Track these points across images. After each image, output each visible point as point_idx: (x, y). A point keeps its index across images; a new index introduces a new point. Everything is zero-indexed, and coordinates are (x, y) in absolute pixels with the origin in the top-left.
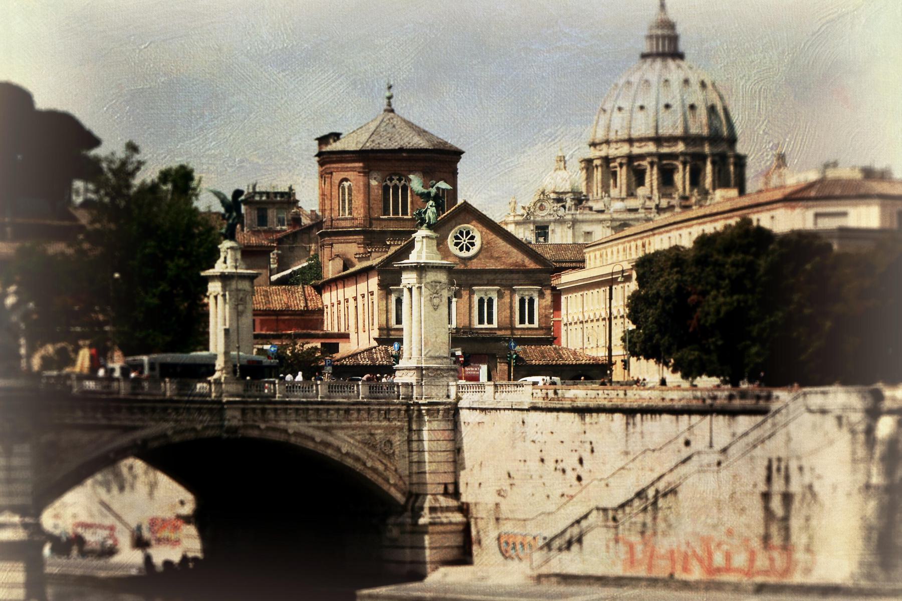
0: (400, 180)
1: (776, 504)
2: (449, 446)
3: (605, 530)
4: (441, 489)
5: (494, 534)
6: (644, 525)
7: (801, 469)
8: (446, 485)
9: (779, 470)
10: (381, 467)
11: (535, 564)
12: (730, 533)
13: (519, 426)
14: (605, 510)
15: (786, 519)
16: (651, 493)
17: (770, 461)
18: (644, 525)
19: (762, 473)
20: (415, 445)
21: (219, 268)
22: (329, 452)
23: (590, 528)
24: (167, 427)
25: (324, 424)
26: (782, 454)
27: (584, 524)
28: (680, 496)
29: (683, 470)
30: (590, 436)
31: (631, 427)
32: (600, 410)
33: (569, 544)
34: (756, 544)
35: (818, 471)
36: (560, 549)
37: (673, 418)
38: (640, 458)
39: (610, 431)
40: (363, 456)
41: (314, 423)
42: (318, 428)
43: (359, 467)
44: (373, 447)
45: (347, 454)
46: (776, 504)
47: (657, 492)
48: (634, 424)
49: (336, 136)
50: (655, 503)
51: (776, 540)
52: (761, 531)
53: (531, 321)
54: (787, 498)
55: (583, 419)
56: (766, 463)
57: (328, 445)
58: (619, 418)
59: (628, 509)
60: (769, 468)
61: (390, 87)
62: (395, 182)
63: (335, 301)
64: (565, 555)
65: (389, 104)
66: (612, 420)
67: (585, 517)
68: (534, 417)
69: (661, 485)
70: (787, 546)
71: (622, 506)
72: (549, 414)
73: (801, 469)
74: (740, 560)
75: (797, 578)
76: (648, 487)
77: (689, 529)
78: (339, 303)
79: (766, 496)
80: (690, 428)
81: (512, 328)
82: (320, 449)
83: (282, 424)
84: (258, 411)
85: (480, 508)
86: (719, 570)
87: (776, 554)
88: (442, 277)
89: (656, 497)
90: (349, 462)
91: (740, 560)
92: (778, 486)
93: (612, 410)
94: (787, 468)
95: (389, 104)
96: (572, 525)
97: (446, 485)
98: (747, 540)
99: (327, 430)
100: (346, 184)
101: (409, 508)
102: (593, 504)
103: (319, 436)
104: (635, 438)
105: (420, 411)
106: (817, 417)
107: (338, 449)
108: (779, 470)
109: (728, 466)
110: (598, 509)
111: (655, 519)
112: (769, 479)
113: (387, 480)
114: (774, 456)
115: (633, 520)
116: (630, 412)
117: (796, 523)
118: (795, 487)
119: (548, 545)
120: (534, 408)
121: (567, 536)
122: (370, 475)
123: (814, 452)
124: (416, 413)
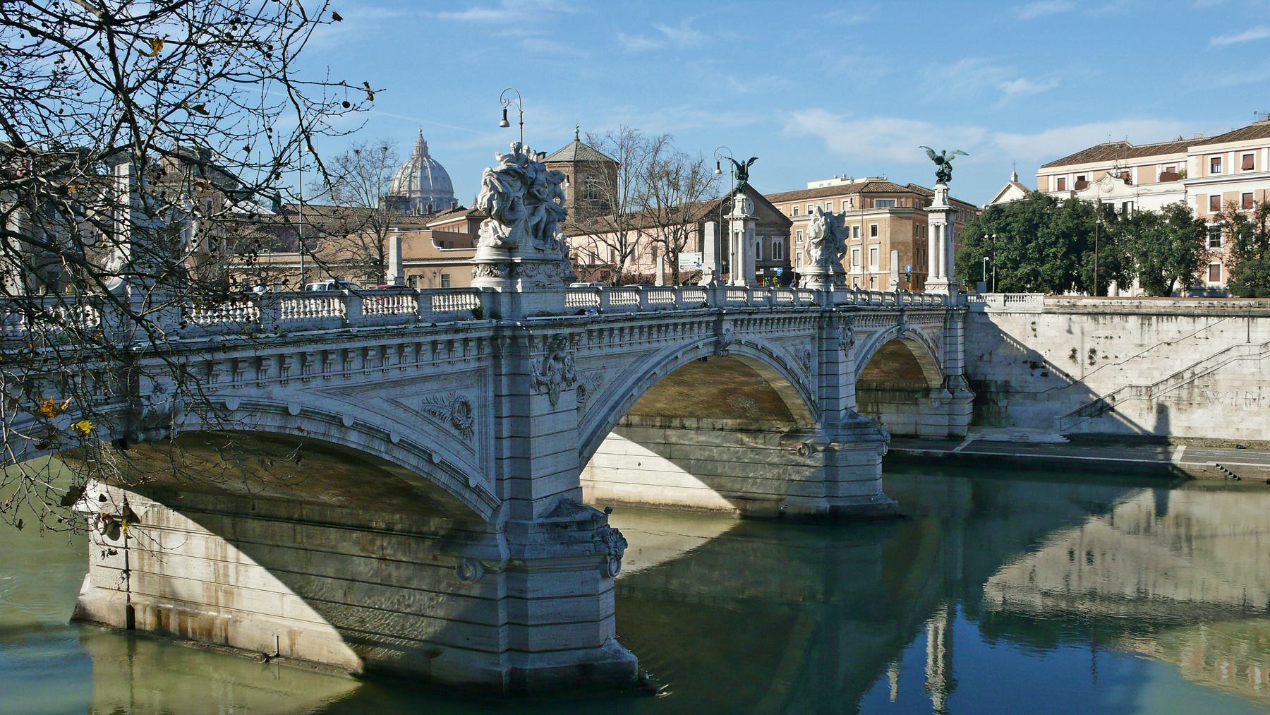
16: (1187, 375)
28: (1217, 377)
29: (1223, 358)
31: (1146, 327)
36: (1091, 416)
47: (1193, 374)
49: (544, 154)
55: (1096, 320)
58: (1132, 319)
59: (1162, 387)
64: (1094, 420)
69: (1198, 370)
72: (1061, 317)
80: (1208, 328)
102: (1126, 382)
110: (1131, 387)
111: (1191, 394)
119: (1079, 413)
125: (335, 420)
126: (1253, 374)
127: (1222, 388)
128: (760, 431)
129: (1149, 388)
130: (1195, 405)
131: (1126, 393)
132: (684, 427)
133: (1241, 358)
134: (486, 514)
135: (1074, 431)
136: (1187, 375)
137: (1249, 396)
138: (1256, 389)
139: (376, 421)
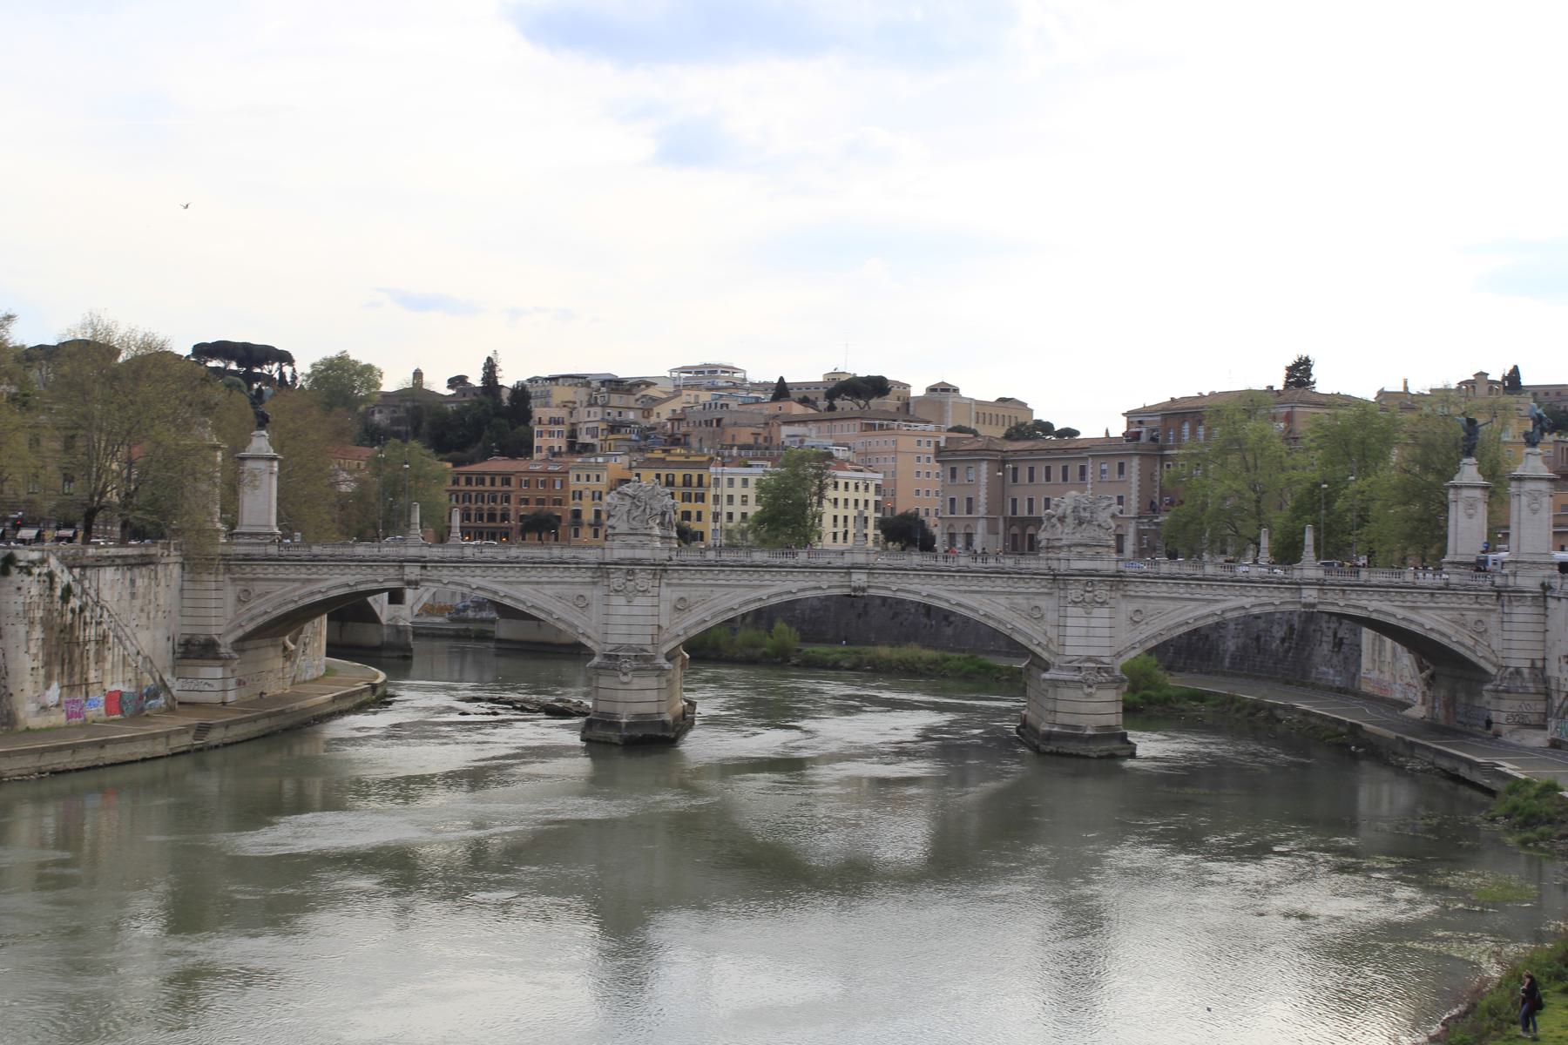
2: (1540, 628)
4: (1528, 663)
8: (1533, 661)
10: (1470, 643)
21: (1457, 481)
22: (1413, 628)
24: (1246, 601)
43: (1445, 641)
44: (1464, 625)
57: (1412, 621)
82: (1404, 625)
83: (1363, 603)
88: (1544, 486)
97: (1533, 661)
99: (1412, 608)
103: (1401, 613)
107: (1422, 625)
113: (1474, 652)
122: (1456, 648)
125: (496, 593)
134: (596, 648)
139: (523, 597)
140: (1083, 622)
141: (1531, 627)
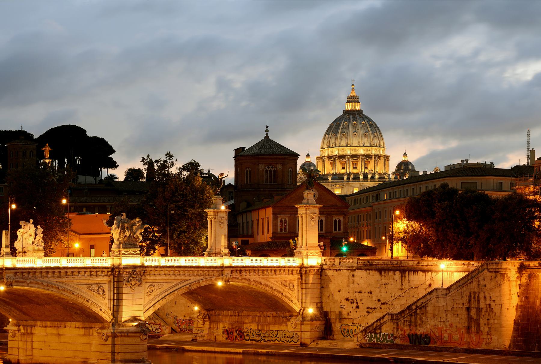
0: (272, 168)
1: (473, 313)
3: (392, 324)
5: (339, 325)
6: (410, 321)
7: (485, 297)
9: (474, 298)
10: (289, 296)
11: (359, 340)
12: (451, 325)
13: (351, 278)
14: (392, 315)
15: (478, 320)
16: (414, 307)
17: (470, 293)
18: (410, 321)
19: (466, 298)
20: (304, 286)
23: (385, 323)
25: (265, 276)
26: (476, 290)
27: (382, 321)
28: (428, 308)
29: (429, 297)
30: (384, 281)
32: (389, 270)
33: (375, 329)
34: (463, 331)
35: (493, 299)
37: (424, 274)
38: (408, 291)
39: (394, 279)
40: (282, 291)
41: (261, 276)
42: (263, 278)
45: (275, 290)
46: (473, 313)
47: (417, 306)
48: (405, 276)
50: (416, 312)
51: (473, 329)
52: (466, 324)
53: (339, 230)
54: (479, 310)
56: (468, 294)
57: (267, 286)
58: (398, 273)
59: (403, 315)
60: (470, 296)
61: (267, 127)
62: (270, 168)
63: (245, 221)
65: (267, 134)
66: (395, 274)
67: (383, 317)
68: (359, 273)
70: (478, 331)
71: (400, 313)
73: (485, 297)
74: (456, 337)
75: (484, 347)
76: (412, 305)
77: (432, 323)
78: (248, 222)
79: (468, 309)
81: (331, 233)
83: (248, 277)
84: (238, 271)
85: (332, 313)
86: (446, 342)
87: (473, 336)
89: (416, 309)
90: (276, 293)
91: (456, 337)
92: (474, 305)
93: (395, 270)
94: (478, 296)
95: (267, 134)
96: (377, 321)
98: (459, 329)
99: (266, 279)
100: (248, 170)
101: (301, 313)
103: (263, 282)
104: (406, 283)
105: (306, 270)
106: (493, 275)
108: (474, 298)
109: (450, 296)
110: (388, 314)
112: (470, 301)
114: (472, 291)
115: (406, 319)
116: (403, 271)
117: (482, 321)
118: (482, 305)
119: (365, 330)
120: (359, 268)
121: (375, 326)
123: (492, 289)
124: (304, 271)
126: (443, 306)
127: (429, 315)
128: (91, 328)
129: (396, 314)
130: (418, 326)
131: (387, 318)
132: (65, 327)
133: (438, 296)
135: (363, 341)
136: (414, 307)
137: (442, 320)
138: (444, 315)
140: (130, 296)
141: (316, 286)
